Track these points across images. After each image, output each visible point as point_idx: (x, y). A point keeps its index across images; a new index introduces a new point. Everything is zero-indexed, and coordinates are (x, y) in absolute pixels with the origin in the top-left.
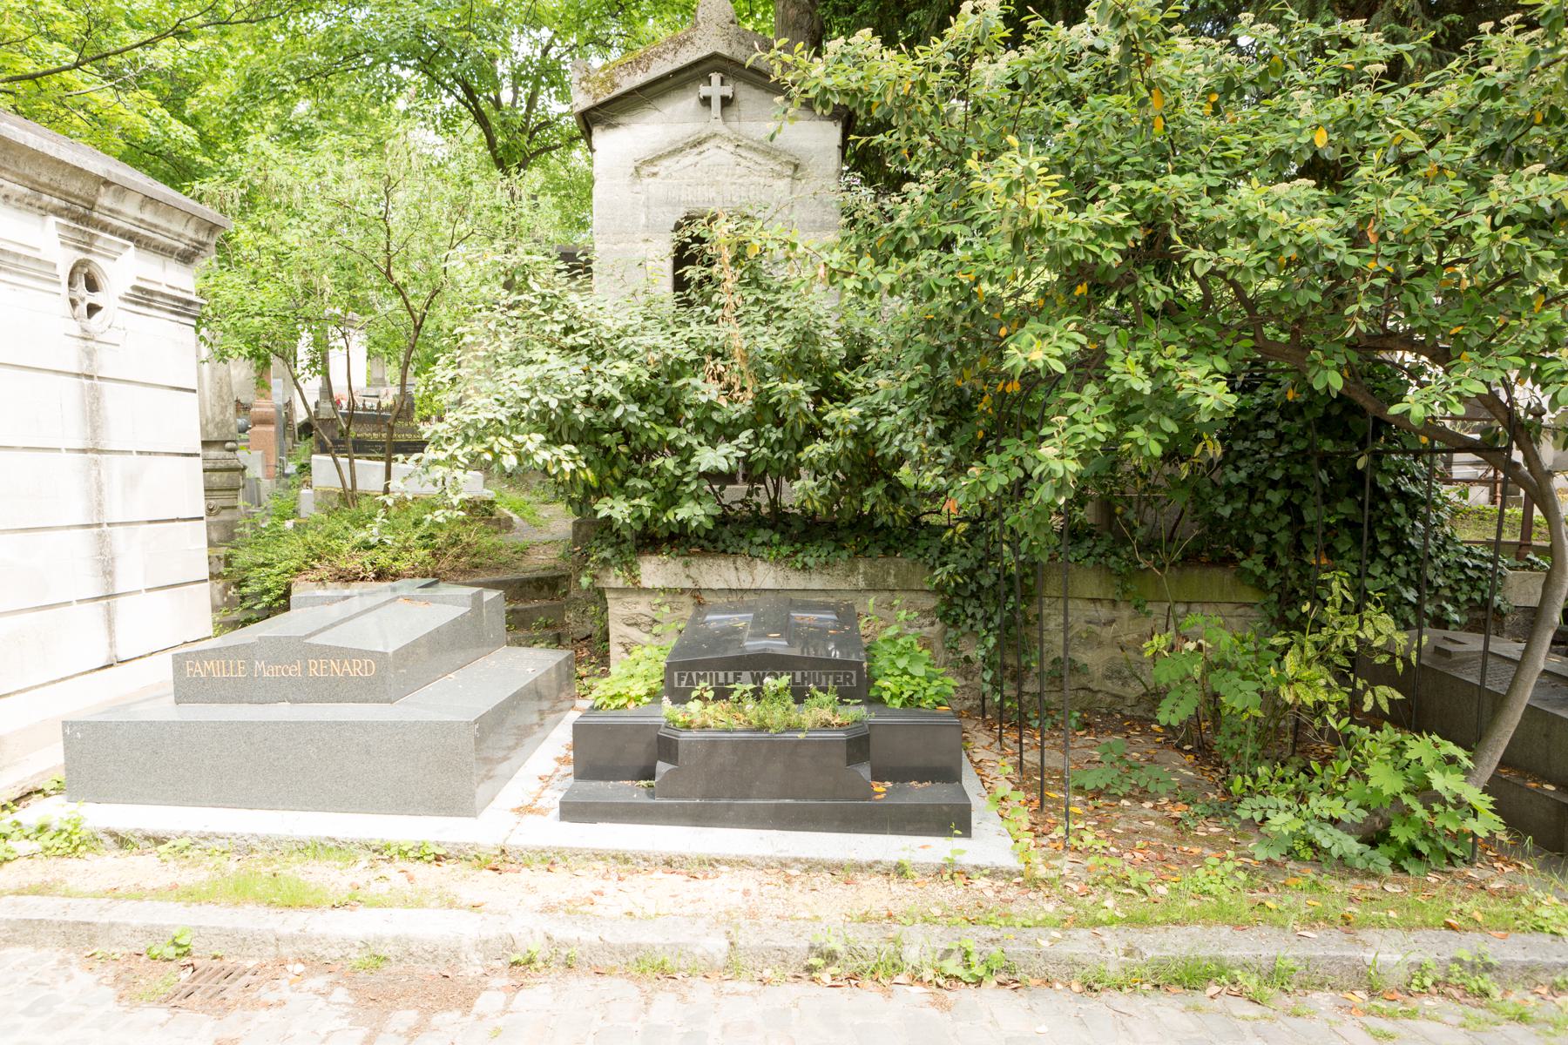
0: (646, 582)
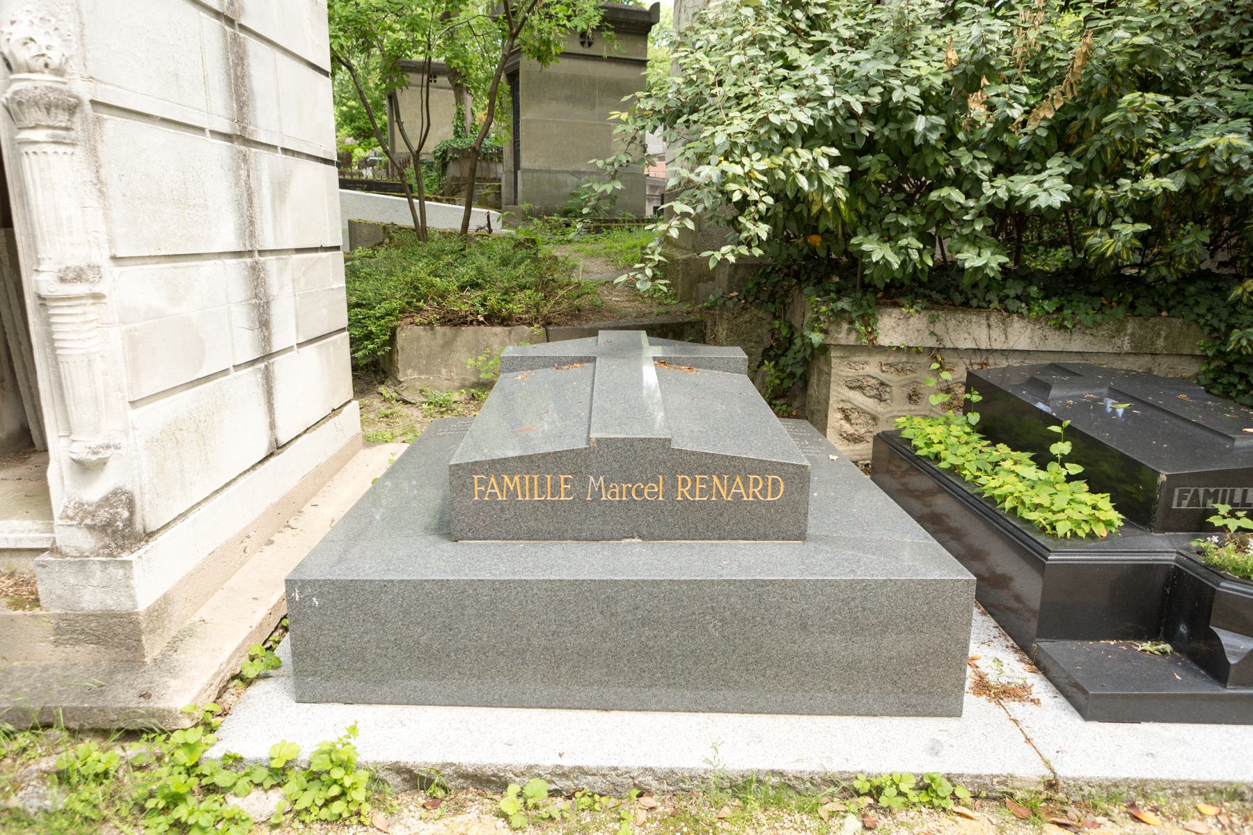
0: (883, 340)
